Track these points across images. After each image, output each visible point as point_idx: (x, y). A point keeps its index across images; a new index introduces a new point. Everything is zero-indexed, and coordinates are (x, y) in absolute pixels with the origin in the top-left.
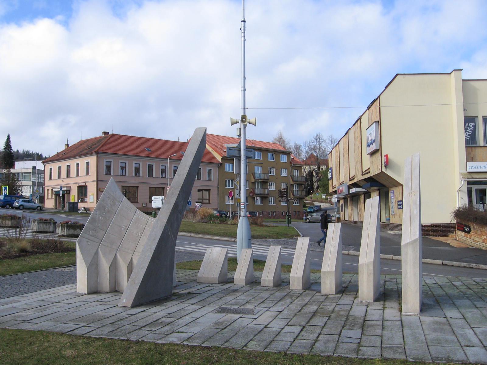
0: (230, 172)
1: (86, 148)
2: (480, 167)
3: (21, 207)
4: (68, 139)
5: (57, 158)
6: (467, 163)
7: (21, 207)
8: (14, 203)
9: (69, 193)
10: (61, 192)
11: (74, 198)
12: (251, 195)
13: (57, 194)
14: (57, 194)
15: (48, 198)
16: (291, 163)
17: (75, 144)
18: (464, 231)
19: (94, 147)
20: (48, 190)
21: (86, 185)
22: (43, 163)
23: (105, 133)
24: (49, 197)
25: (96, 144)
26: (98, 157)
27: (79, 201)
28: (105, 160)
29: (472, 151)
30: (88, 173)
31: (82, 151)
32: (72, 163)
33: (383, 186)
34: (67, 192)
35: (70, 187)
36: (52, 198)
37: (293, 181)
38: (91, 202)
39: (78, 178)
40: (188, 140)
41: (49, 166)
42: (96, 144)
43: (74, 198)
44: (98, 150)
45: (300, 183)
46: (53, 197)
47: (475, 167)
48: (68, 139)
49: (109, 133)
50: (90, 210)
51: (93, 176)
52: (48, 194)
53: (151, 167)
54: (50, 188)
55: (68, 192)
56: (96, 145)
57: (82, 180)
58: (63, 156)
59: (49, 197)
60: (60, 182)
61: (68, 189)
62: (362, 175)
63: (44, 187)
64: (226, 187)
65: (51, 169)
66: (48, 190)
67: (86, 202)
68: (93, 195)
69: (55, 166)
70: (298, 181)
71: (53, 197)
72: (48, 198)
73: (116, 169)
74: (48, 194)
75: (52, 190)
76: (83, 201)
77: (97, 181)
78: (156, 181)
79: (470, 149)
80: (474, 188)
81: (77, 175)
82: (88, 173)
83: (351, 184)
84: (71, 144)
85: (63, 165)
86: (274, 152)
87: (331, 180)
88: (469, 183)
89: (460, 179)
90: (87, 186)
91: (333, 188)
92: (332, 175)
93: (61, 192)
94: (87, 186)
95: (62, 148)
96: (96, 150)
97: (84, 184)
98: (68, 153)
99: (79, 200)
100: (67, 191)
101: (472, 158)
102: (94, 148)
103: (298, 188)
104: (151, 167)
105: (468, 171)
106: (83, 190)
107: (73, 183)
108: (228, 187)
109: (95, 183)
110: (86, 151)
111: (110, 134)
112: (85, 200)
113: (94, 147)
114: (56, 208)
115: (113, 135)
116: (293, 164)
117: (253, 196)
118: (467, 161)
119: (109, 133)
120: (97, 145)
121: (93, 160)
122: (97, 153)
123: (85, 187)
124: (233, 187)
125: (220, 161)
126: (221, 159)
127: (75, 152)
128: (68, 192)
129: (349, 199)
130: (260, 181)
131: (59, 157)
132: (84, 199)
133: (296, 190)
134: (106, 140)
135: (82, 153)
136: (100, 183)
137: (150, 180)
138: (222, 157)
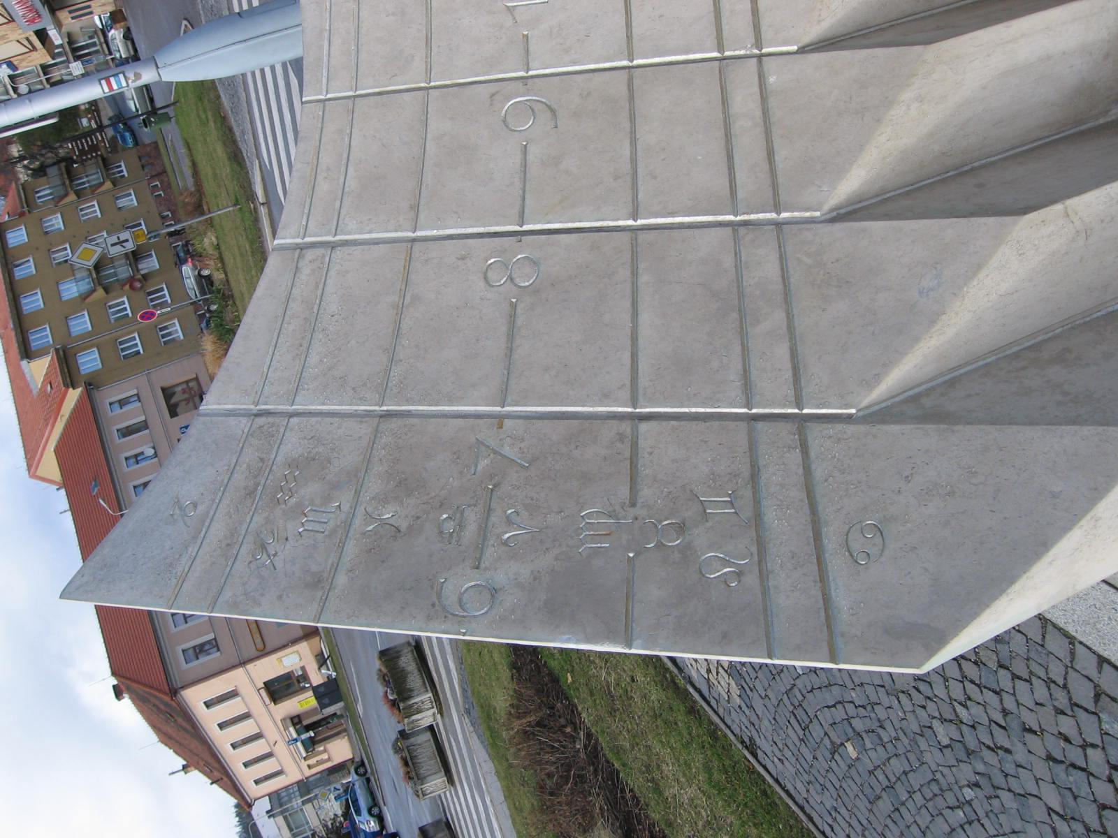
0: (100, 356)
1: (172, 724)
3: (375, 811)
4: (170, 774)
5: (225, 779)
7: (375, 811)
8: (372, 830)
9: (298, 716)
10: (304, 736)
11: (304, 702)
12: (138, 285)
13: (310, 745)
14: (310, 745)
15: (329, 759)
17: (175, 751)
19: (162, 707)
20: (309, 767)
21: (263, 686)
22: (250, 806)
24: (325, 756)
26: (183, 688)
27: (307, 685)
28: (182, 667)
30: (233, 694)
31: (185, 729)
32: (222, 740)
34: (297, 724)
35: (283, 720)
36: (325, 751)
37: (66, 195)
38: (298, 659)
39: (254, 712)
40: (58, 489)
41: (252, 790)
43: (304, 702)
44: (165, 693)
45: (66, 176)
46: (322, 748)
48: (170, 774)
49: (114, 687)
50: (319, 651)
52: (319, 763)
54: (304, 764)
55: (296, 720)
56: (157, 703)
57: (255, 700)
58: (215, 768)
59: (325, 756)
60: (282, 750)
61: (289, 722)
63: (306, 778)
64: (142, 352)
65: (257, 782)
66: (309, 767)
67: (303, 668)
68: (280, 659)
69: (246, 777)
70: (64, 184)
71: (322, 748)
72: (329, 759)
74: (319, 763)
75: (305, 759)
76: (304, 677)
77: (243, 663)
81: (247, 716)
82: (233, 694)
84: (181, 762)
85: (235, 760)
86: (10, 266)
90: (264, 683)
93: (304, 736)
94: (264, 683)
95: (196, 776)
96: (167, 699)
97: (263, 693)
98: (203, 760)
99: (304, 688)
100: (294, 725)
102: (166, 704)
103: (81, 178)
106: (278, 689)
107: (273, 719)
109: (250, 667)
110: (180, 720)
111: (115, 682)
112: (300, 673)
113: (162, 707)
114: (345, 730)
115: (114, 673)
116: (23, 208)
117: (139, 281)
119: (114, 687)
120: (152, 699)
121: (195, 697)
122: (174, 692)
123: (268, 685)
124: (136, 335)
125: (80, 389)
126: (74, 389)
127: (194, 744)
128: (296, 720)
130: (95, 276)
131: (222, 775)
132: (299, 676)
133: (88, 182)
134: (134, 685)
135: (189, 727)
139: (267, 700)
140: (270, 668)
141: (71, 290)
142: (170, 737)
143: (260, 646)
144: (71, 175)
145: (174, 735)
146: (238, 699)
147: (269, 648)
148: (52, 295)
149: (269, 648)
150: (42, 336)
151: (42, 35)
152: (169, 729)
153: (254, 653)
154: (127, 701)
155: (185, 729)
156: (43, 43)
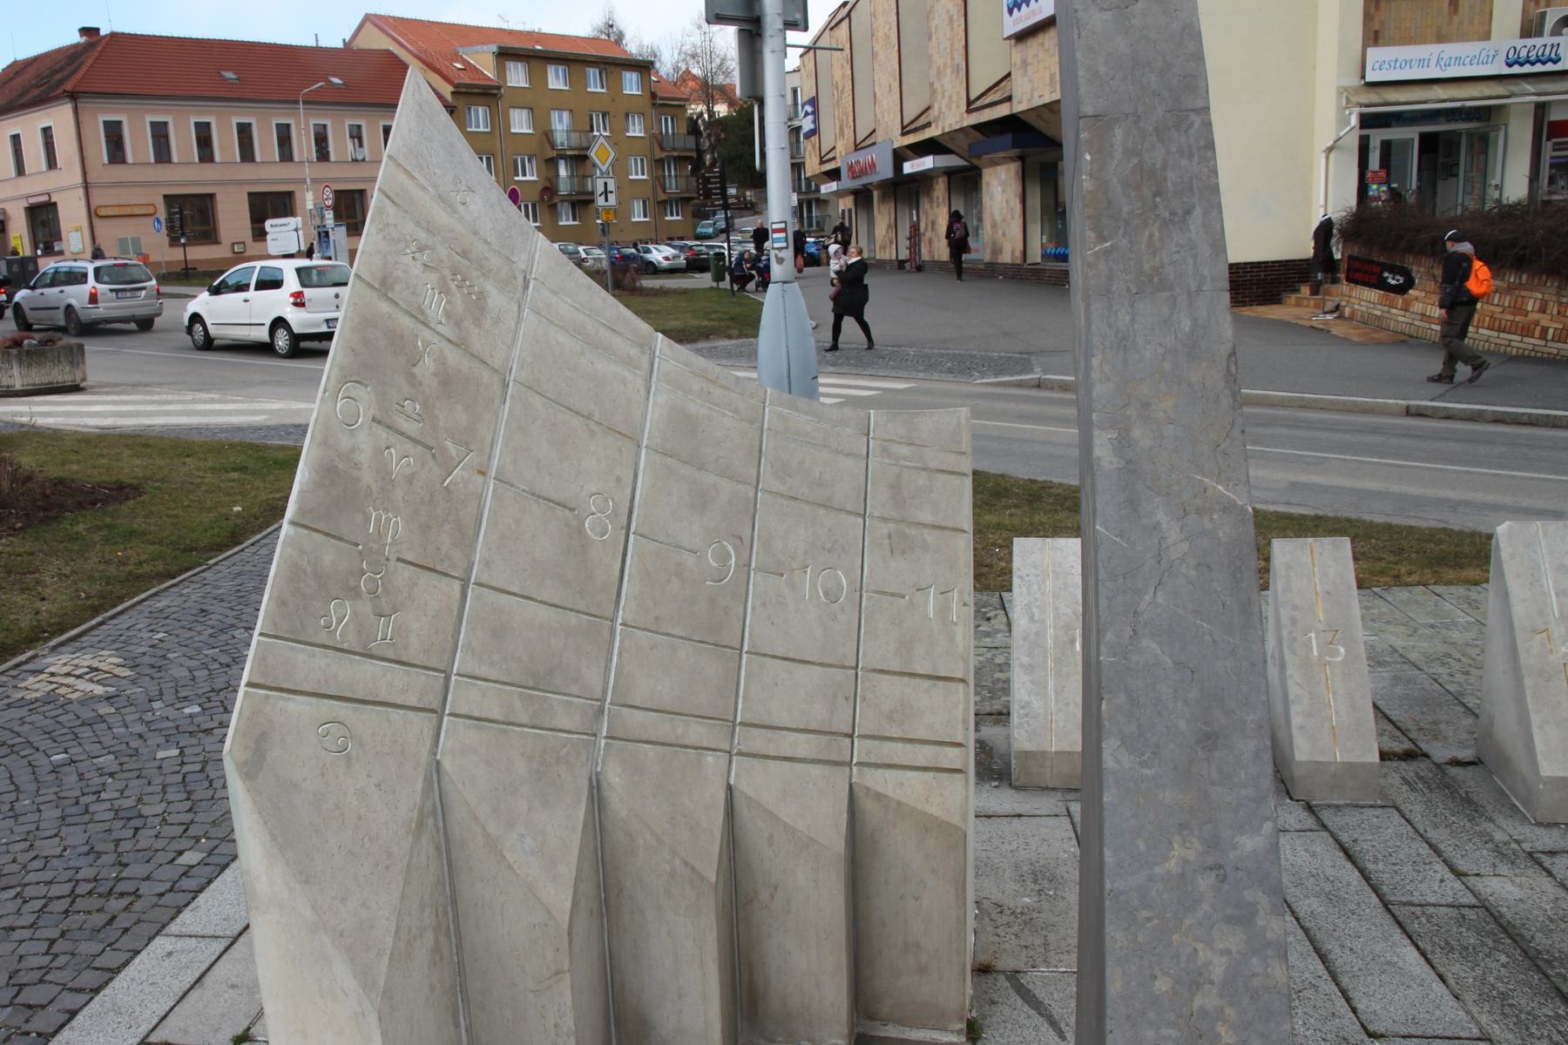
6: (1369, 50)
16: (653, 95)
18: (1382, 285)
19: (59, 76)
23: (85, 31)
25: (62, 69)
26: (76, 111)
28: (99, 116)
30: (52, 163)
39: (22, 180)
42: (62, 69)
47: (1395, 63)
51: (69, 172)
53: (244, 131)
56: (65, 73)
57: (38, 184)
62: (969, 111)
67: (61, 253)
68: (79, 229)
70: (674, 149)
73: (138, 144)
76: (49, 251)
77: (86, 186)
78: (269, 173)
82: (52, 163)
83: (910, 147)
87: (815, 139)
88: (1367, 121)
89: (1341, 110)
91: (822, 162)
92: (816, 121)
97: (45, 198)
99: (36, 248)
101: (1376, 33)
102: (61, 82)
104: (244, 131)
105: (1371, 77)
106: (43, 216)
108: (520, 178)
109: (81, 192)
110: (35, 93)
111: (103, 33)
113: (59, 76)
115: (113, 35)
120: (69, 69)
121: (59, 117)
122: (73, 96)
123: (50, 207)
129: (875, 194)
135: (25, 99)
136: (94, 192)
137: (248, 172)
138: (456, 86)
139: (33, 200)
140: (72, 215)
141: (560, 124)
142: (17, 73)
143: (103, 212)
144: (680, 160)
145: (19, 80)
146: (44, 167)
147: (96, 221)
148: (558, 101)
149: (96, 221)
150: (517, 76)
151: (834, 175)
152: (29, 75)
153: (94, 204)
154: (75, 38)
156: (826, 173)
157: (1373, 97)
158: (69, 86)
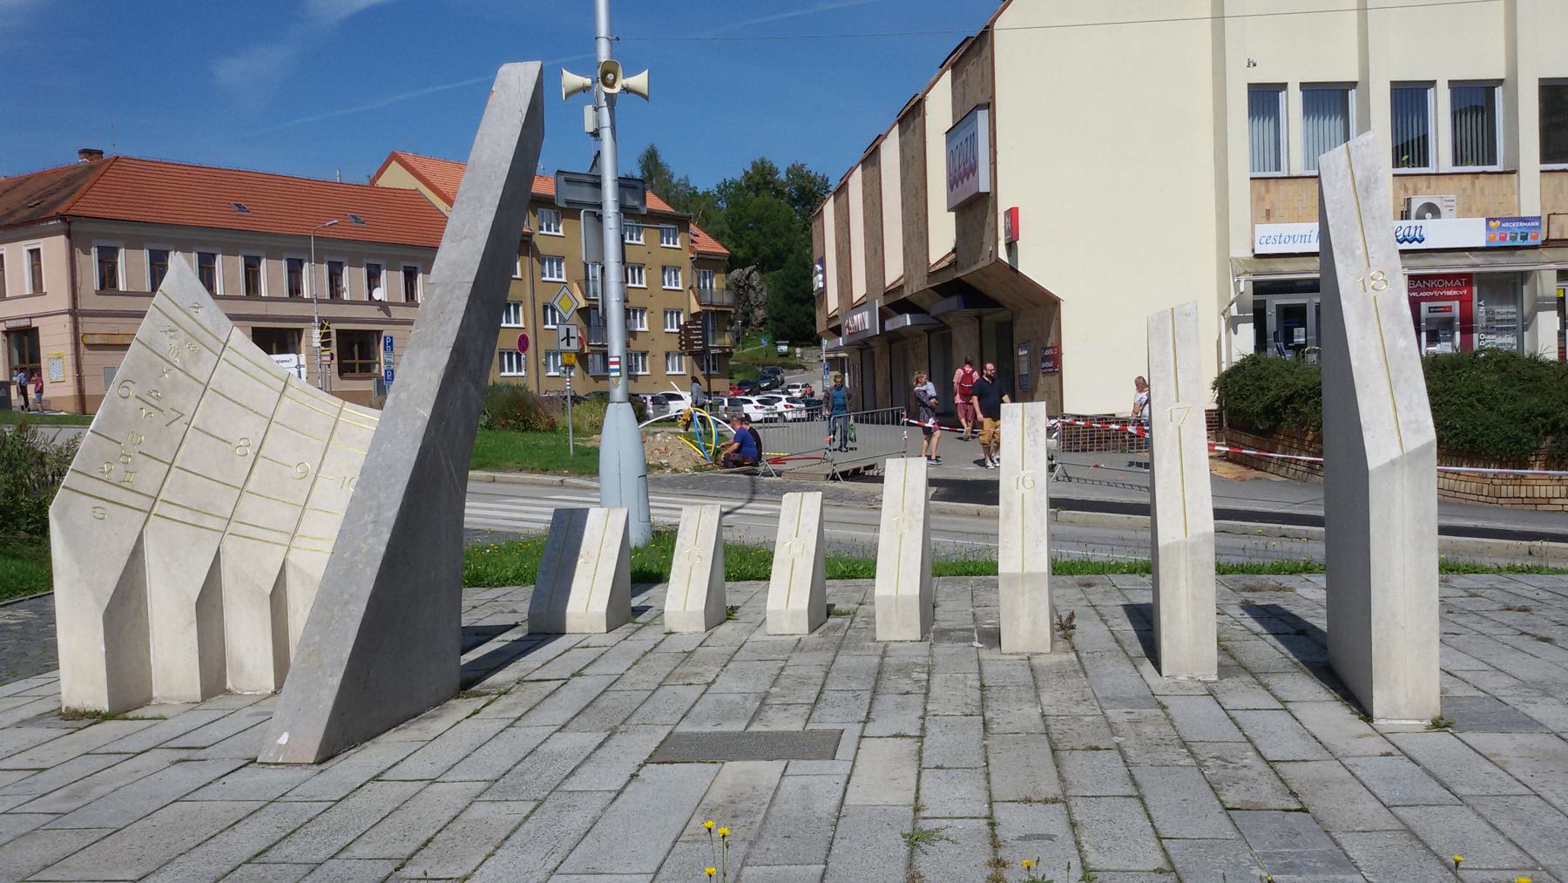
2: (1292, 238)
19: (53, 198)
23: (87, 152)
29: (1267, 190)
30: (37, 288)
33: (995, 304)
47: (1279, 239)
79: (1260, 185)
80: (1274, 302)
82: (37, 288)
88: (1260, 288)
102: (56, 204)
106: (25, 340)
110: (25, 213)
113: (53, 198)
118: (1255, 221)
124: (521, 325)
135: (12, 220)
140: (55, 342)
155: (11, 214)
157: (1262, 266)
158: (61, 209)
